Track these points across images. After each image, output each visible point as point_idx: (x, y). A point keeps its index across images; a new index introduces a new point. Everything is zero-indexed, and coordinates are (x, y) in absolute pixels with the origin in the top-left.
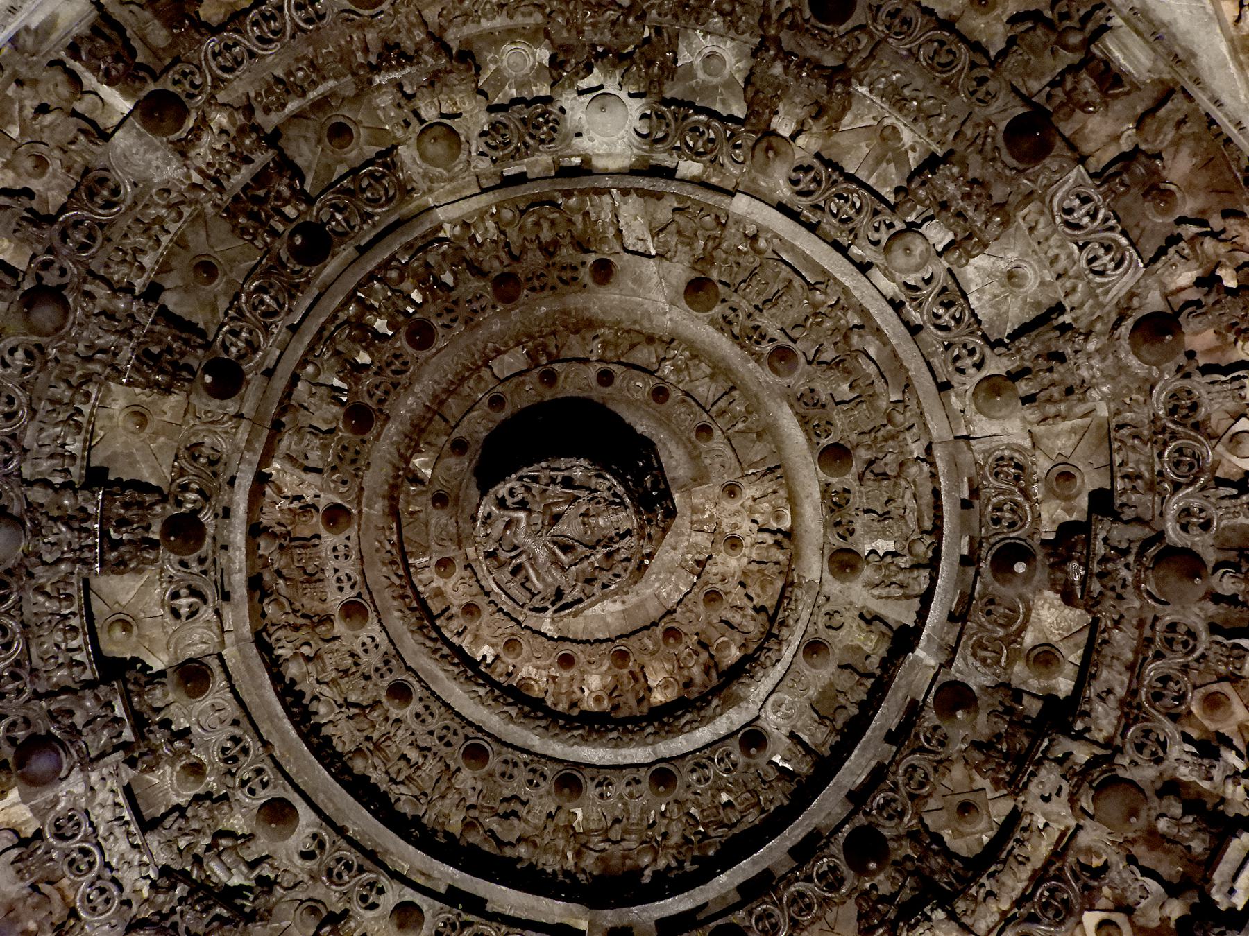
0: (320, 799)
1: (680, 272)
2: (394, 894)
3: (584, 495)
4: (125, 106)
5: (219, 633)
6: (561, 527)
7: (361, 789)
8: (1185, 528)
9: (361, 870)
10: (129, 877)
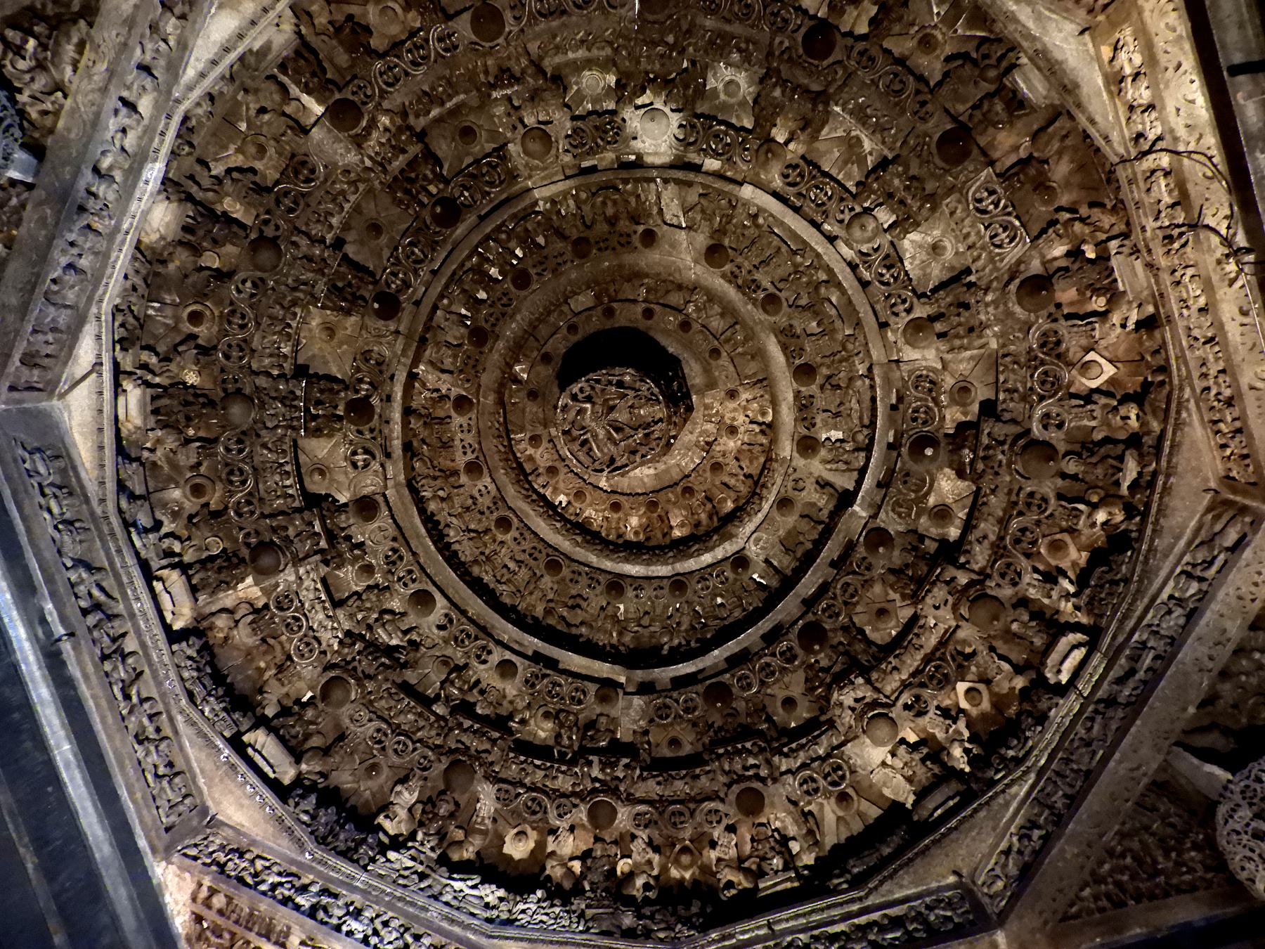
0: (450, 593)
1: (702, 239)
3: (631, 393)
4: (319, 110)
6: (614, 415)
7: (477, 586)
8: (1045, 427)
9: (476, 638)
10: (325, 636)
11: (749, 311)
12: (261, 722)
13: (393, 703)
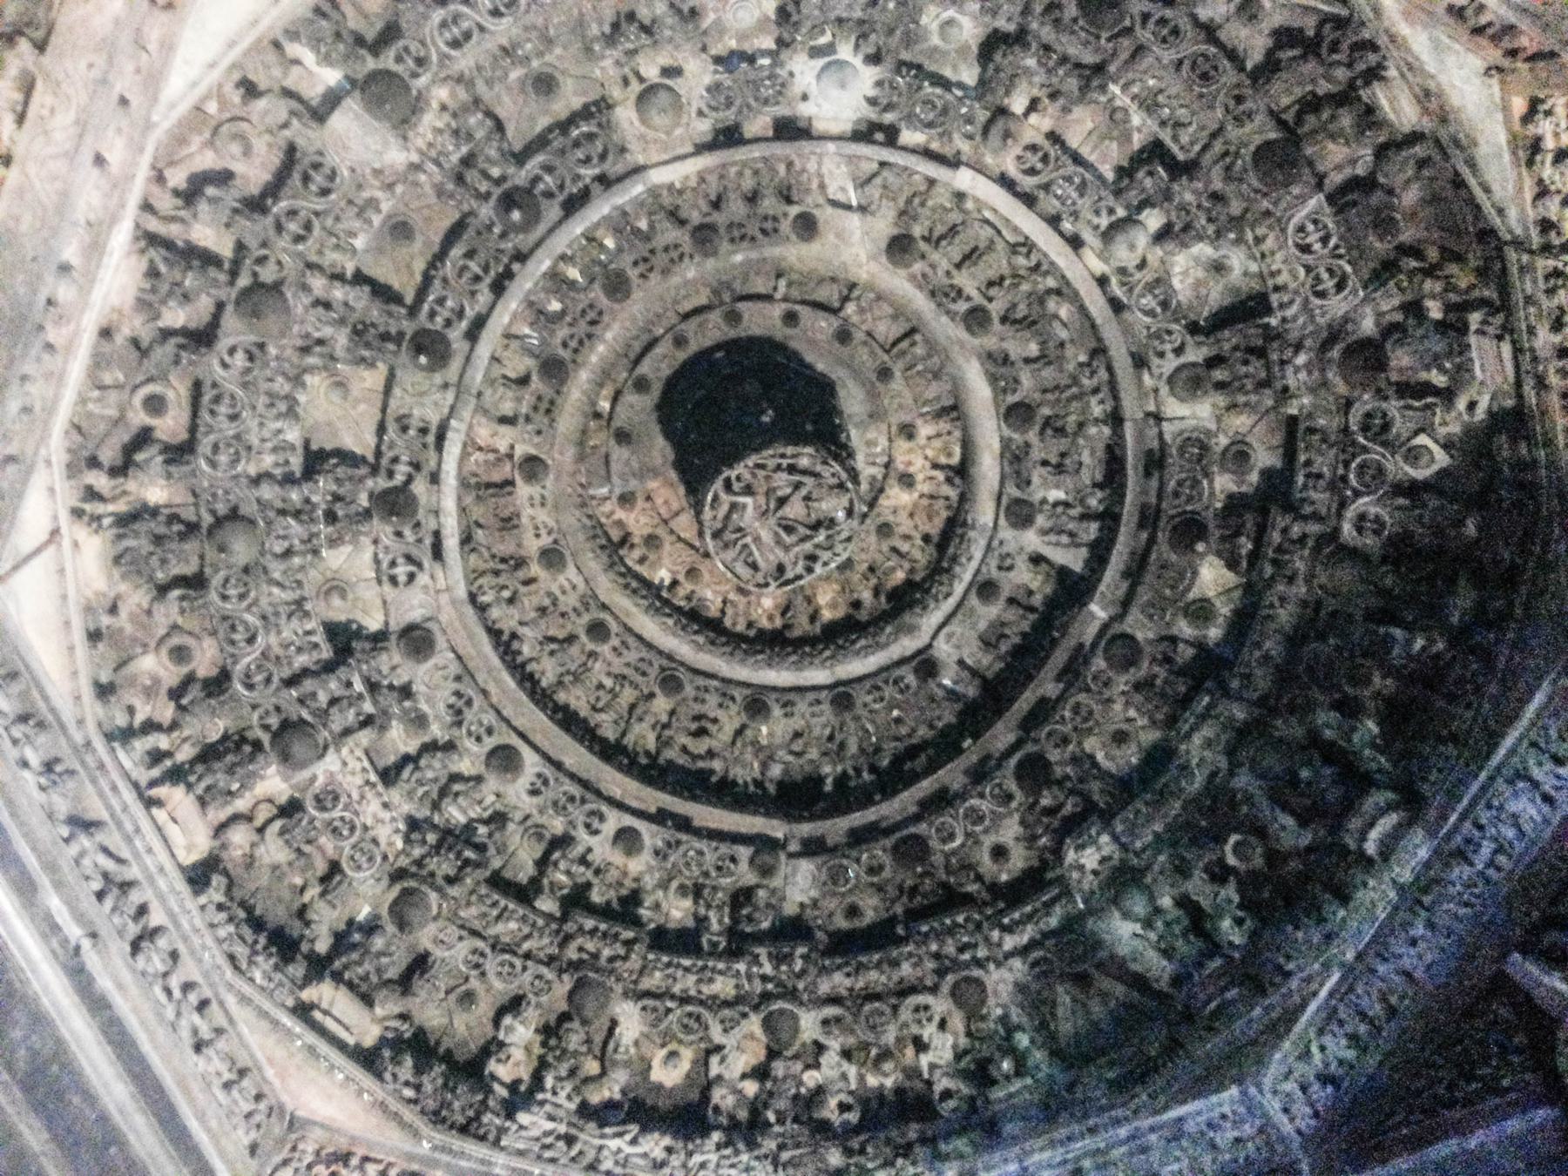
0: (537, 738)
1: (884, 225)
2: (614, 821)
3: (809, 481)
5: (436, 596)
7: (568, 720)
8: (1360, 530)
9: (583, 801)
10: (383, 833)
11: (946, 329)
12: (319, 967)
13: (484, 909)
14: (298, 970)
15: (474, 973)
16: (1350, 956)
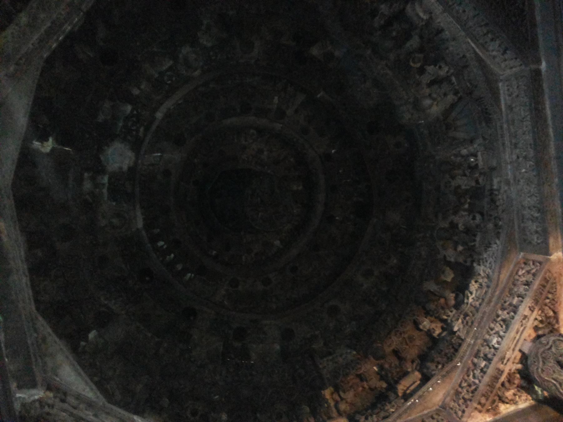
10: (350, 357)
12: (392, 387)
14: (392, 396)
15: (403, 335)
16: (463, 33)
